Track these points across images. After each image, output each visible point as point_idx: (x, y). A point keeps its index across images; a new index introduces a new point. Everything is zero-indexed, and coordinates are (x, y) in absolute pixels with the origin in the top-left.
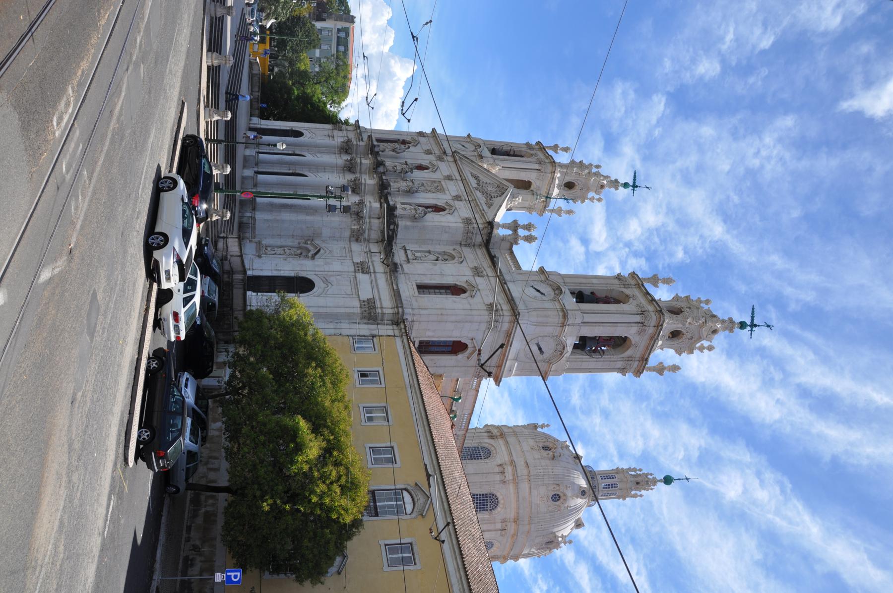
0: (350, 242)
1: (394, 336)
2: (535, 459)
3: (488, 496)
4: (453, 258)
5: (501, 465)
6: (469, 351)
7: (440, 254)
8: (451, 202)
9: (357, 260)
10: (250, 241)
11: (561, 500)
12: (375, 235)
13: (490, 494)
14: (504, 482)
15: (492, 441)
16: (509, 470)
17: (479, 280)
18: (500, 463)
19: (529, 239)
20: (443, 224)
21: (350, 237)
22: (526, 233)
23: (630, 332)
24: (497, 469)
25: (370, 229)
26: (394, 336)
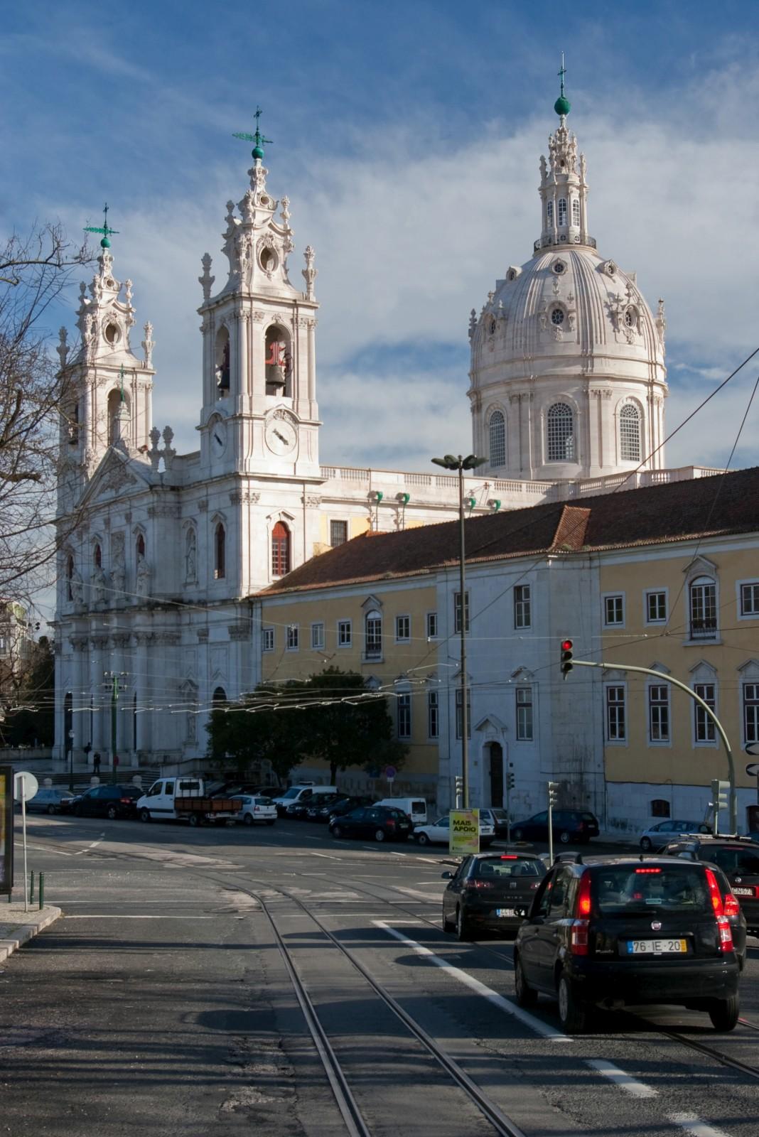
0: (180, 645)
1: (261, 607)
2: (505, 347)
3: (551, 418)
4: (191, 530)
5: (511, 399)
6: (284, 519)
7: (189, 544)
8: (133, 526)
9: (196, 639)
10: (184, 754)
11: (561, 308)
12: (170, 618)
13: (549, 415)
14: (532, 395)
15: (484, 408)
16: (518, 388)
17: (212, 506)
18: (507, 401)
19: (168, 434)
20: (156, 541)
21: (176, 646)
22: (161, 440)
23: (260, 331)
24: (516, 406)
25: (165, 625)
26: (261, 607)
